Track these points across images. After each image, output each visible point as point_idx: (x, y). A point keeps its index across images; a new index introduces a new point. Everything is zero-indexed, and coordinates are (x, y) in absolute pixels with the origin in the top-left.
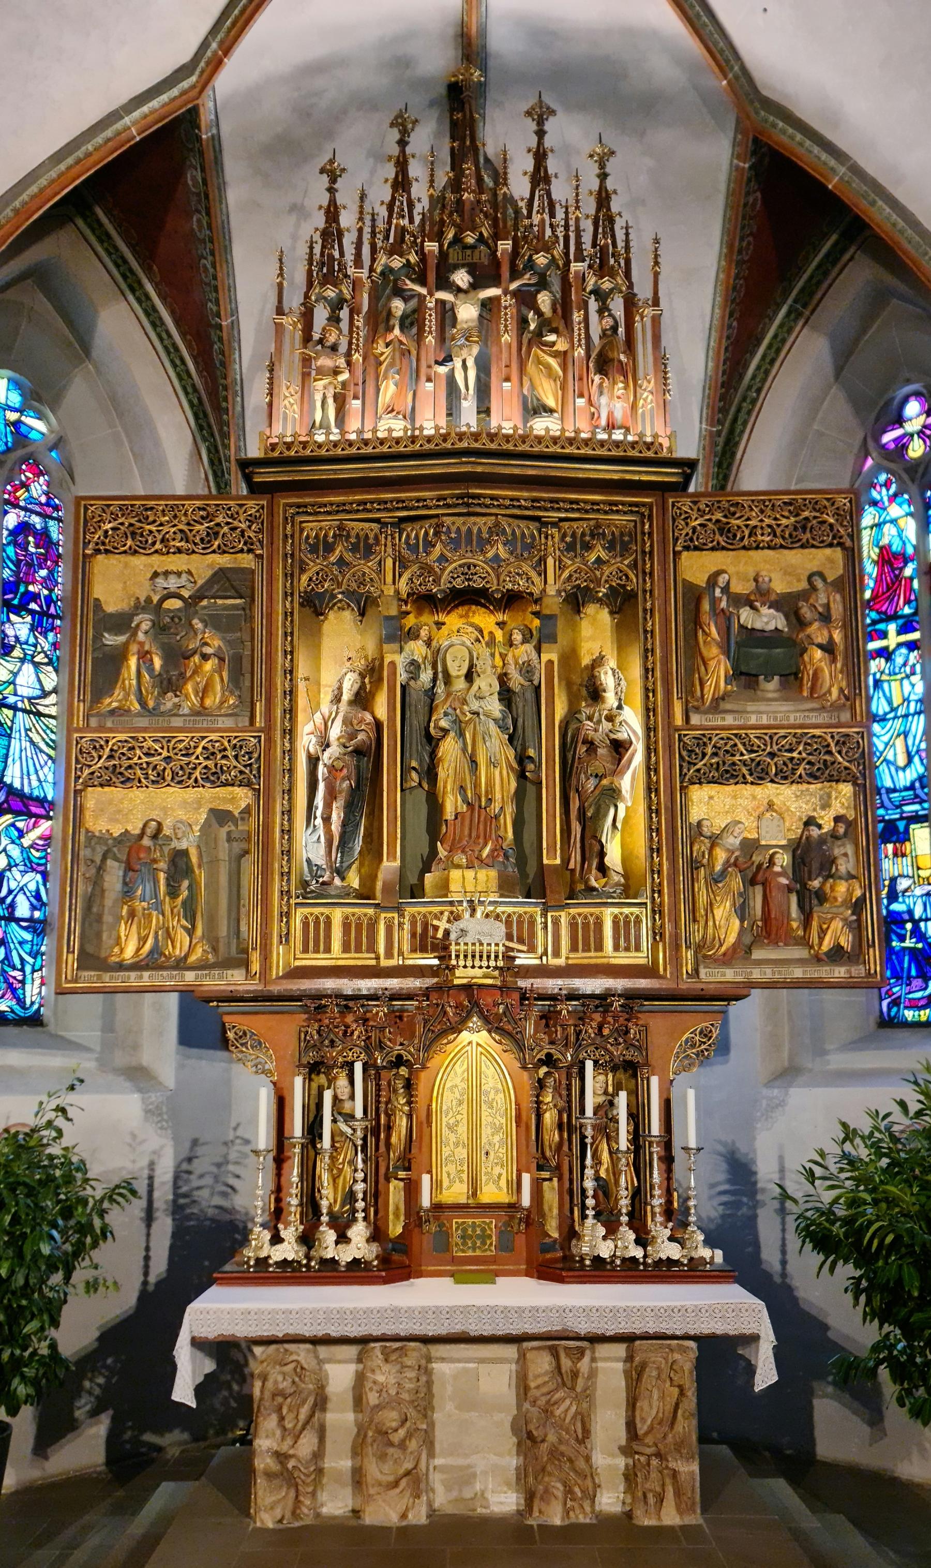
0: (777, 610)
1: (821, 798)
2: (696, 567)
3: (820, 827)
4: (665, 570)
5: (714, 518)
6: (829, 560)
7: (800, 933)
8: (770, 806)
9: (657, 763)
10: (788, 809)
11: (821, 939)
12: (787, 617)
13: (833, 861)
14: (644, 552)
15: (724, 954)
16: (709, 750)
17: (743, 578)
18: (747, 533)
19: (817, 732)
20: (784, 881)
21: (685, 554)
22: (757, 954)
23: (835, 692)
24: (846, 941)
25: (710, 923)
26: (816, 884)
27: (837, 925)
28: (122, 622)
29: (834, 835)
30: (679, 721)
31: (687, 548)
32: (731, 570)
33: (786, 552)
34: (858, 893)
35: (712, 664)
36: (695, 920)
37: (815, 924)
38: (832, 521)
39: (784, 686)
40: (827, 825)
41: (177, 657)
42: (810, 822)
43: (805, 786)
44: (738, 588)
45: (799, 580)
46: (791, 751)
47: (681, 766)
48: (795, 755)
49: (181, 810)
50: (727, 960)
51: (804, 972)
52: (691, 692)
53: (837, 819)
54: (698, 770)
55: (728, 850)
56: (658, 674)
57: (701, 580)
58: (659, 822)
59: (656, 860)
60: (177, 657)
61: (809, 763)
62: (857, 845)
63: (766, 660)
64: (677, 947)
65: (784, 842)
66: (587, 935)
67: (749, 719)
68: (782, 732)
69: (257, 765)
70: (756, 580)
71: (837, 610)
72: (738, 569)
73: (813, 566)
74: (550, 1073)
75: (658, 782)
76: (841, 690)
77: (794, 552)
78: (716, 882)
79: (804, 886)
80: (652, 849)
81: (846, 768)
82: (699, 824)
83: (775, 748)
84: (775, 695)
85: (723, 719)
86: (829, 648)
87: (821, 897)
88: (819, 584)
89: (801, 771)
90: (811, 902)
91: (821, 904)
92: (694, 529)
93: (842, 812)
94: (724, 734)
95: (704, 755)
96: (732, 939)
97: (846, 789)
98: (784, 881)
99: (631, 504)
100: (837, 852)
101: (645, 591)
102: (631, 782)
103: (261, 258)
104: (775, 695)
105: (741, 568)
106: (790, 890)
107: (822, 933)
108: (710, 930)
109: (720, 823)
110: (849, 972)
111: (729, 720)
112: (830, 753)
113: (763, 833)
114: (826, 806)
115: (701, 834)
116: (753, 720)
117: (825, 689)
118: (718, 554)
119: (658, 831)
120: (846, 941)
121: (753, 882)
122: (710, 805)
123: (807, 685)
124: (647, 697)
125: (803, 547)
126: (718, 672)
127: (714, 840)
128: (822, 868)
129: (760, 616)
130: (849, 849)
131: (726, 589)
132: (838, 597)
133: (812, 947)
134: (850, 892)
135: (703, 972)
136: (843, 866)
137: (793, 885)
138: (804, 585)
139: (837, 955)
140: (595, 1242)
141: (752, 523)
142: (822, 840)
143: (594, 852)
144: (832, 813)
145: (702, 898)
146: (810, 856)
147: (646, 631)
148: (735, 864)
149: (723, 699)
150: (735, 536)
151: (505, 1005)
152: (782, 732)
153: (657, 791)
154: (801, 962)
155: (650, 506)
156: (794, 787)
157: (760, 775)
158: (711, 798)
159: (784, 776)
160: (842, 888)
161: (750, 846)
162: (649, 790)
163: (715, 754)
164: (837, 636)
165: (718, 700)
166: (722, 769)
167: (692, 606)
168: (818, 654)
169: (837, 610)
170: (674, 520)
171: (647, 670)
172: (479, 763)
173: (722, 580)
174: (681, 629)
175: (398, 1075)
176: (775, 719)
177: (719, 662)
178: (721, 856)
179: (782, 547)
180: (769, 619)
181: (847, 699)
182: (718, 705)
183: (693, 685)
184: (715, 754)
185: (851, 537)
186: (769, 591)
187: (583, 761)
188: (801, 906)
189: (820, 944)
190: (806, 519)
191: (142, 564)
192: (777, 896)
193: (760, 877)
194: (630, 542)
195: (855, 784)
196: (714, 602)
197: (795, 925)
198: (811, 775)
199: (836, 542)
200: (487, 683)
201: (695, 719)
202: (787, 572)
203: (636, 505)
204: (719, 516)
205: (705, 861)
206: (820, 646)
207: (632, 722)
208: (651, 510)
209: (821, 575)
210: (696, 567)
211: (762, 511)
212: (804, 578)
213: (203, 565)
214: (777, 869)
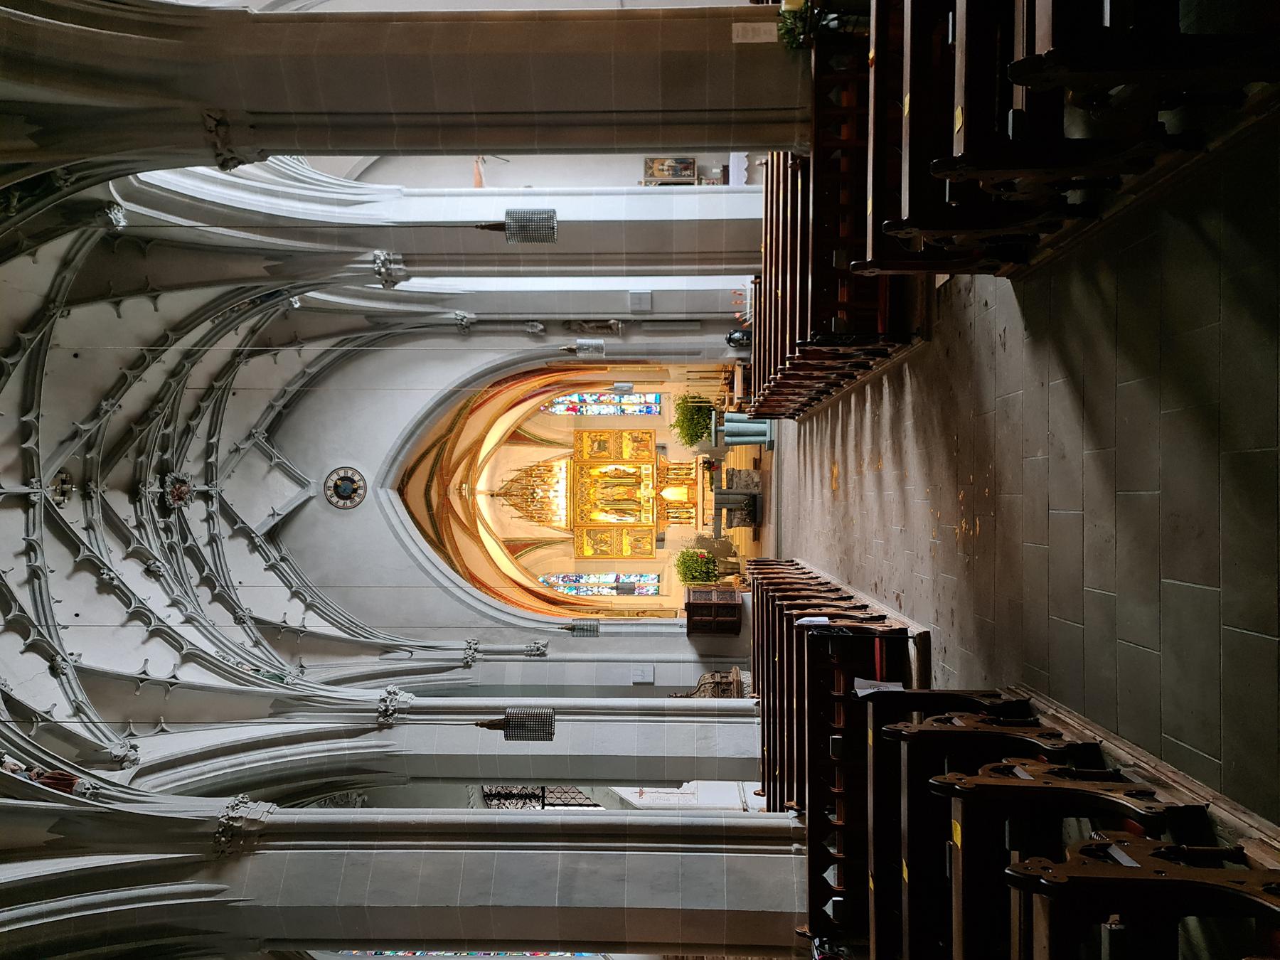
2: (586, 457)
6: (585, 435)
28: (596, 550)
41: (601, 541)
49: (626, 540)
60: (601, 541)
63: (602, 446)
66: (647, 475)
69: (620, 527)
72: (587, 449)
74: (669, 483)
103: (523, 530)
122: (626, 456)
140: (693, 476)
146: (635, 440)
151: (658, 489)
172: (620, 492)
175: (669, 504)
180: (596, 445)
187: (618, 475)
191: (585, 547)
200: (605, 491)
207: (612, 467)
210: (586, 457)
213: (585, 538)
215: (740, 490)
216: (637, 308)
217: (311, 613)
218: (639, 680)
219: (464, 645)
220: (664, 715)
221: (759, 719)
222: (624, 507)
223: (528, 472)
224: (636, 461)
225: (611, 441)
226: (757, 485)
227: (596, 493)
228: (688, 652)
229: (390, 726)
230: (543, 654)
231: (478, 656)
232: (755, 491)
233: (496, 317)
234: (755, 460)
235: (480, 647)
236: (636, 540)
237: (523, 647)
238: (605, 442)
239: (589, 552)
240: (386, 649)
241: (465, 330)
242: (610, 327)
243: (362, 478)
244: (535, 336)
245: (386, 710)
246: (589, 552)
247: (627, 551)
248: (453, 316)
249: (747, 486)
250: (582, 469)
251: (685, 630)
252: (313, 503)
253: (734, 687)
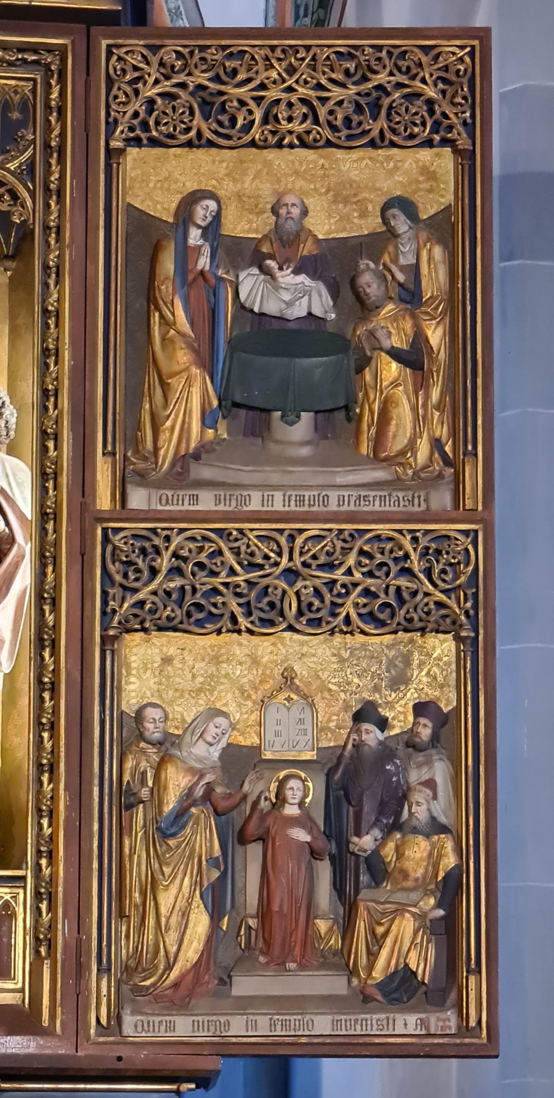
0: (314, 276)
1: (391, 663)
2: (155, 181)
3: (383, 724)
4: (86, 189)
5: (191, 82)
6: (424, 175)
7: (335, 942)
8: (288, 679)
9: (57, 587)
10: (324, 688)
11: (372, 956)
12: (335, 292)
13: (402, 796)
14: (47, 146)
15: (176, 985)
16: (165, 562)
17: (249, 204)
18: (258, 115)
19: (383, 529)
20: (301, 835)
21: (133, 152)
22: (243, 986)
23: (423, 450)
24: (422, 961)
25: (151, 921)
26: (366, 842)
27: (406, 926)
29: (411, 742)
30: (104, 501)
31: (137, 142)
32: (226, 189)
33: (339, 154)
34: (450, 861)
35: (177, 383)
36: (122, 915)
37: (361, 926)
38: (431, 93)
39: (322, 430)
40: (400, 718)
42: (366, 714)
43: (360, 638)
44: (238, 225)
45: (363, 214)
46: (330, 567)
47: (105, 593)
48: (338, 574)
50: (180, 997)
51: (335, 1023)
52: (134, 442)
53: (421, 709)
54: (141, 603)
55: (191, 770)
56: (65, 402)
57: (163, 207)
58: (55, 711)
59: (47, 788)
61: (367, 592)
62: (455, 763)
63: (286, 378)
64: (80, 970)
65: (309, 755)
67: (246, 500)
68: (314, 529)
70: (275, 211)
71: (434, 280)
72: (243, 185)
73: (393, 186)
75: (56, 627)
76: (437, 444)
77: (355, 155)
78: (165, 835)
79: (343, 844)
80: (40, 766)
81: (440, 605)
82: (139, 716)
83: (298, 560)
84: (305, 451)
85: (195, 499)
86: (414, 358)
87: (377, 869)
88: (401, 224)
89: (349, 608)
90: (355, 875)
91: (378, 884)
92: (151, 102)
93: (432, 693)
94: (197, 529)
95: (154, 572)
96: (192, 951)
97: (443, 647)
98: (301, 835)
99: (22, 48)
100: (414, 776)
101: (46, 228)
104: (305, 451)
105: (248, 184)
106: (315, 854)
107: (376, 942)
108: (150, 936)
109: (185, 710)
110: (424, 1023)
111: (206, 502)
112: (407, 572)
113: (270, 736)
114: (399, 681)
115: (141, 737)
116: (255, 503)
117: (400, 443)
118: (201, 154)
119: (53, 727)
120: (422, 961)
121: (243, 839)
122: (158, 673)
123: (368, 432)
124: (44, 449)
125: (372, 144)
126: (188, 405)
127: (168, 746)
128: (382, 809)
129: (277, 288)
130: (440, 771)
131: (212, 230)
132: (438, 251)
133: (353, 973)
134: (434, 859)
135: (129, 1022)
136: (420, 808)
137: (322, 843)
138: (373, 224)
139: (401, 988)
141: (272, 94)
142: (386, 752)
144: (412, 696)
145: (137, 869)
146: (360, 785)
147: (45, 312)
148: (208, 795)
149: (196, 456)
150: (233, 120)
152: (314, 529)
153: (54, 644)
154: (328, 1003)
155: (62, 52)
156: (338, 638)
157: (267, 615)
158: (167, 660)
159: (313, 618)
160: (419, 849)
161: (240, 761)
162: (40, 643)
163: (176, 571)
164: (435, 336)
165: (184, 460)
166: (189, 600)
167: (144, 264)
168: (392, 369)
169: (434, 280)
170: (110, 82)
171: (45, 393)
173: (204, 211)
174: (119, 309)
176: (300, 500)
177: (189, 382)
178: (177, 782)
179: (329, 144)
180: (296, 296)
181: (447, 461)
182: (186, 470)
183: (138, 426)
184: (176, 571)
185: (469, 127)
186: (300, 234)
188: (339, 886)
189: (370, 967)
190: (380, 87)
192: (289, 866)
193: (252, 828)
194: (22, 124)
195: (458, 639)
196: (185, 255)
197: (322, 926)
198: (370, 617)
199: (440, 135)
201: (138, 499)
202: (342, 195)
203: (34, 49)
204: (202, 78)
205: (144, 793)
206: (395, 354)
208: (63, 60)
209: (406, 206)
210: (155, 181)
211: (291, 70)
212: (374, 209)
214: (291, 810)
223: (156, 118)
225: (345, 489)
238: (339, 416)
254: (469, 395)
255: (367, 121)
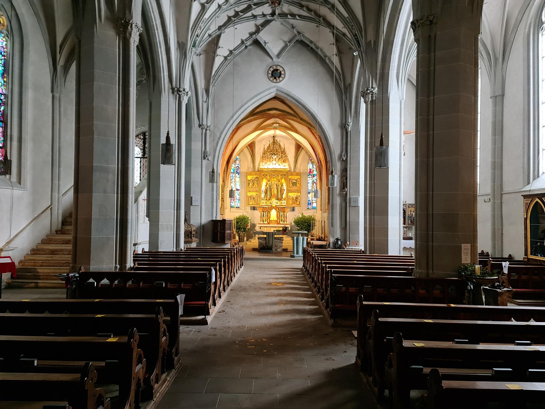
2: (290, 177)
6: (299, 177)
28: (250, 181)
41: (254, 183)
49: (254, 194)
60: (254, 183)
63: (294, 184)
66: (282, 203)
69: (259, 191)
72: (293, 177)
74: (278, 212)
102: (285, 192)
103: (259, 150)
122: (290, 194)
143: (282, 197)
146: (297, 198)
151: (276, 208)
175: (269, 212)
180: (295, 181)
187: (282, 191)
207: (285, 188)
210: (290, 177)
213: (255, 176)
215: (274, 243)
216: (352, 200)
217: (223, 59)
218: (193, 199)
219: (209, 125)
220: (177, 210)
221: (175, 251)
222: (268, 193)
223: (283, 152)
224: (288, 198)
225: (296, 188)
226: (276, 250)
227: (274, 181)
228: (205, 220)
229: (173, 93)
230: (204, 158)
231: (204, 131)
232: (274, 250)
233: (349, 140)
234: (287, 249)
235: (208, 131)
236: (254, 198)
237: (208, 150)
239: (249, 178)
240: (207, 91)
241: (344, 127)
242: (344, 188)
243: (280, 81)
244: (340, 156)
245: (180, 91)
246: (249, 178)
247: (249, 194)
248: (350, 121)
249: (276, 246)
250: (285, 175)
251: (214, 219)
252: (270, 60)
253: (190, 239)
254: (300, 184)
255: (297, 175)
